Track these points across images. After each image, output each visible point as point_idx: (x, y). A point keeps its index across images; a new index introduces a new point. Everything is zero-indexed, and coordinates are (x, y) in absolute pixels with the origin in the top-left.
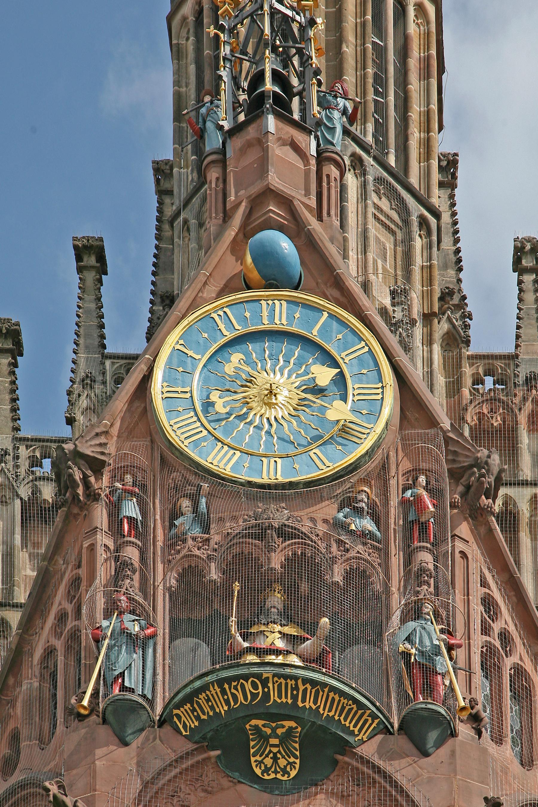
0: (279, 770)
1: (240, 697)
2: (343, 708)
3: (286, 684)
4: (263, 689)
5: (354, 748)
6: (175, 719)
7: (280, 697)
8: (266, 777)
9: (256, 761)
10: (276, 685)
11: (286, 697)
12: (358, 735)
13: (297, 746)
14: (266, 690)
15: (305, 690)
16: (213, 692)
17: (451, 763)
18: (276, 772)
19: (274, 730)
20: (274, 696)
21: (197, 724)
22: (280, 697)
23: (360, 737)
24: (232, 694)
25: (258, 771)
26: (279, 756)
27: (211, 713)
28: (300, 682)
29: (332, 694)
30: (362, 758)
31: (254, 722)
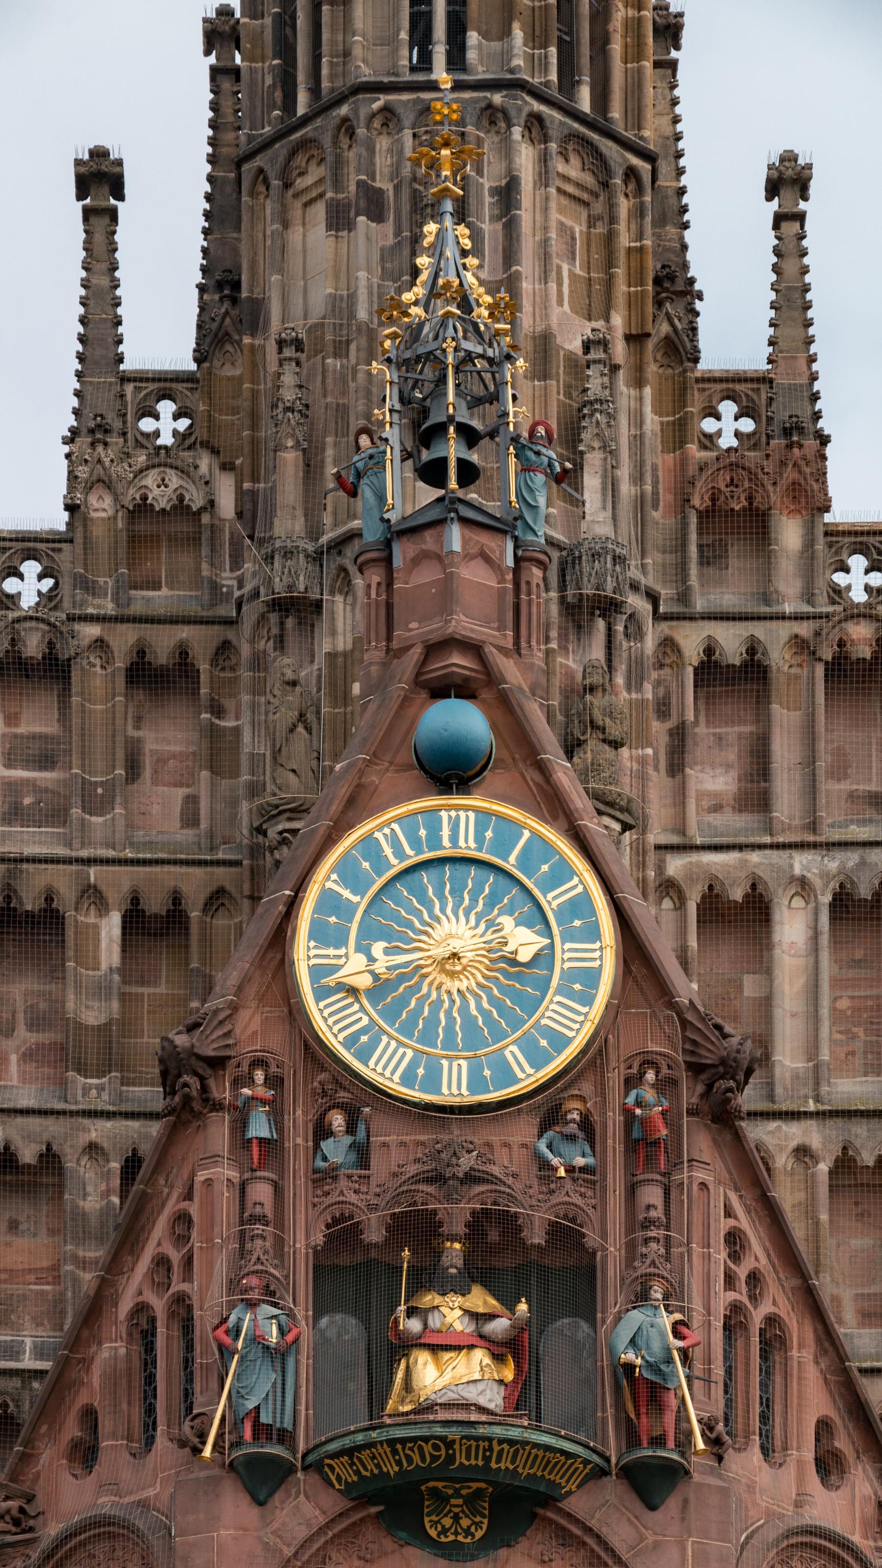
3: (478, 1447)
7: (468, 1458)
8: (443, 1539)
11: (476, 1458)
18: (456, 1533)
20: (461, 1459)
25: (433, 1533)
28: (495, 1443)
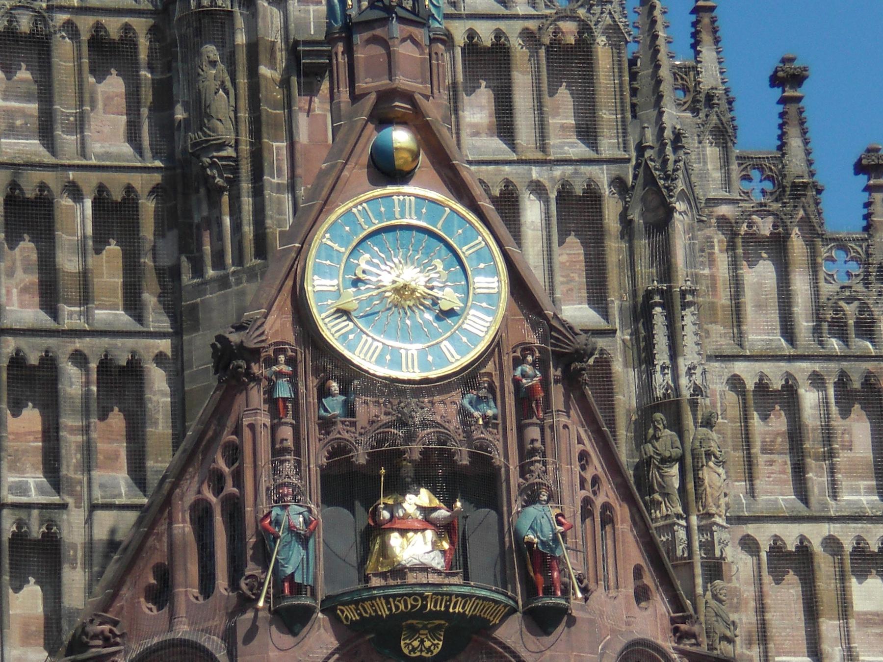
13: (442, 633)
18: (421, 651)
22: (435, 606)
25: (406, 651)
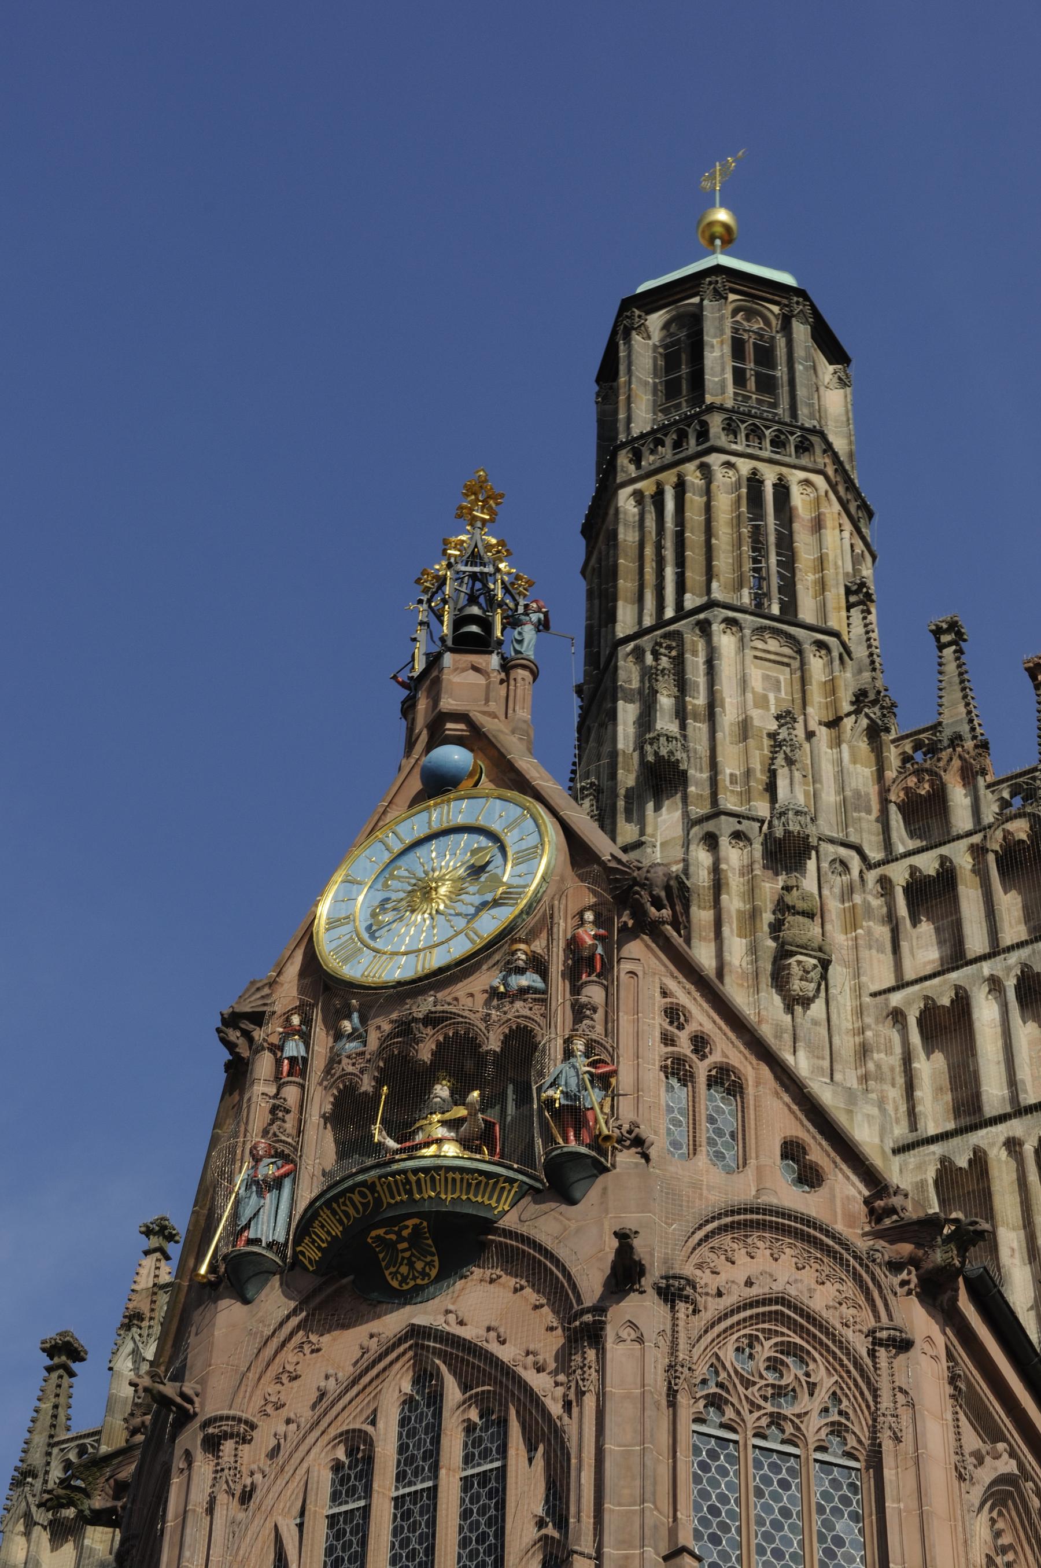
0: (417, 1274)
1: (351, 1211)
2: (469, 1185)
4: (373, 1195)
5: (496, 1222)
6: (301, 1257)
8: (405, 1287)
9: (390, 1274)
10: (385, 1187)
12: (496, 1207)
13: (430, 1242)
14: (376, 1195)
15: (418, 1181)
16: (325, 1216)
17: (602, 1203)
18: (414, 1278)
19: (398, 1234)
20: (387, 1200)
21: (320, 1255)
22: (393, 1197)
23: (500, 1209)
24: (342, 1211)
25: (395, 1284)
26: (414, 1259)
27: (329, 1239)
29: (450, 1175)
30: (504, 1230)
31: (373, 1234)
